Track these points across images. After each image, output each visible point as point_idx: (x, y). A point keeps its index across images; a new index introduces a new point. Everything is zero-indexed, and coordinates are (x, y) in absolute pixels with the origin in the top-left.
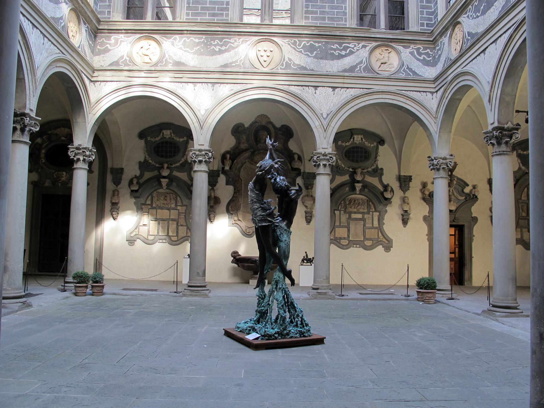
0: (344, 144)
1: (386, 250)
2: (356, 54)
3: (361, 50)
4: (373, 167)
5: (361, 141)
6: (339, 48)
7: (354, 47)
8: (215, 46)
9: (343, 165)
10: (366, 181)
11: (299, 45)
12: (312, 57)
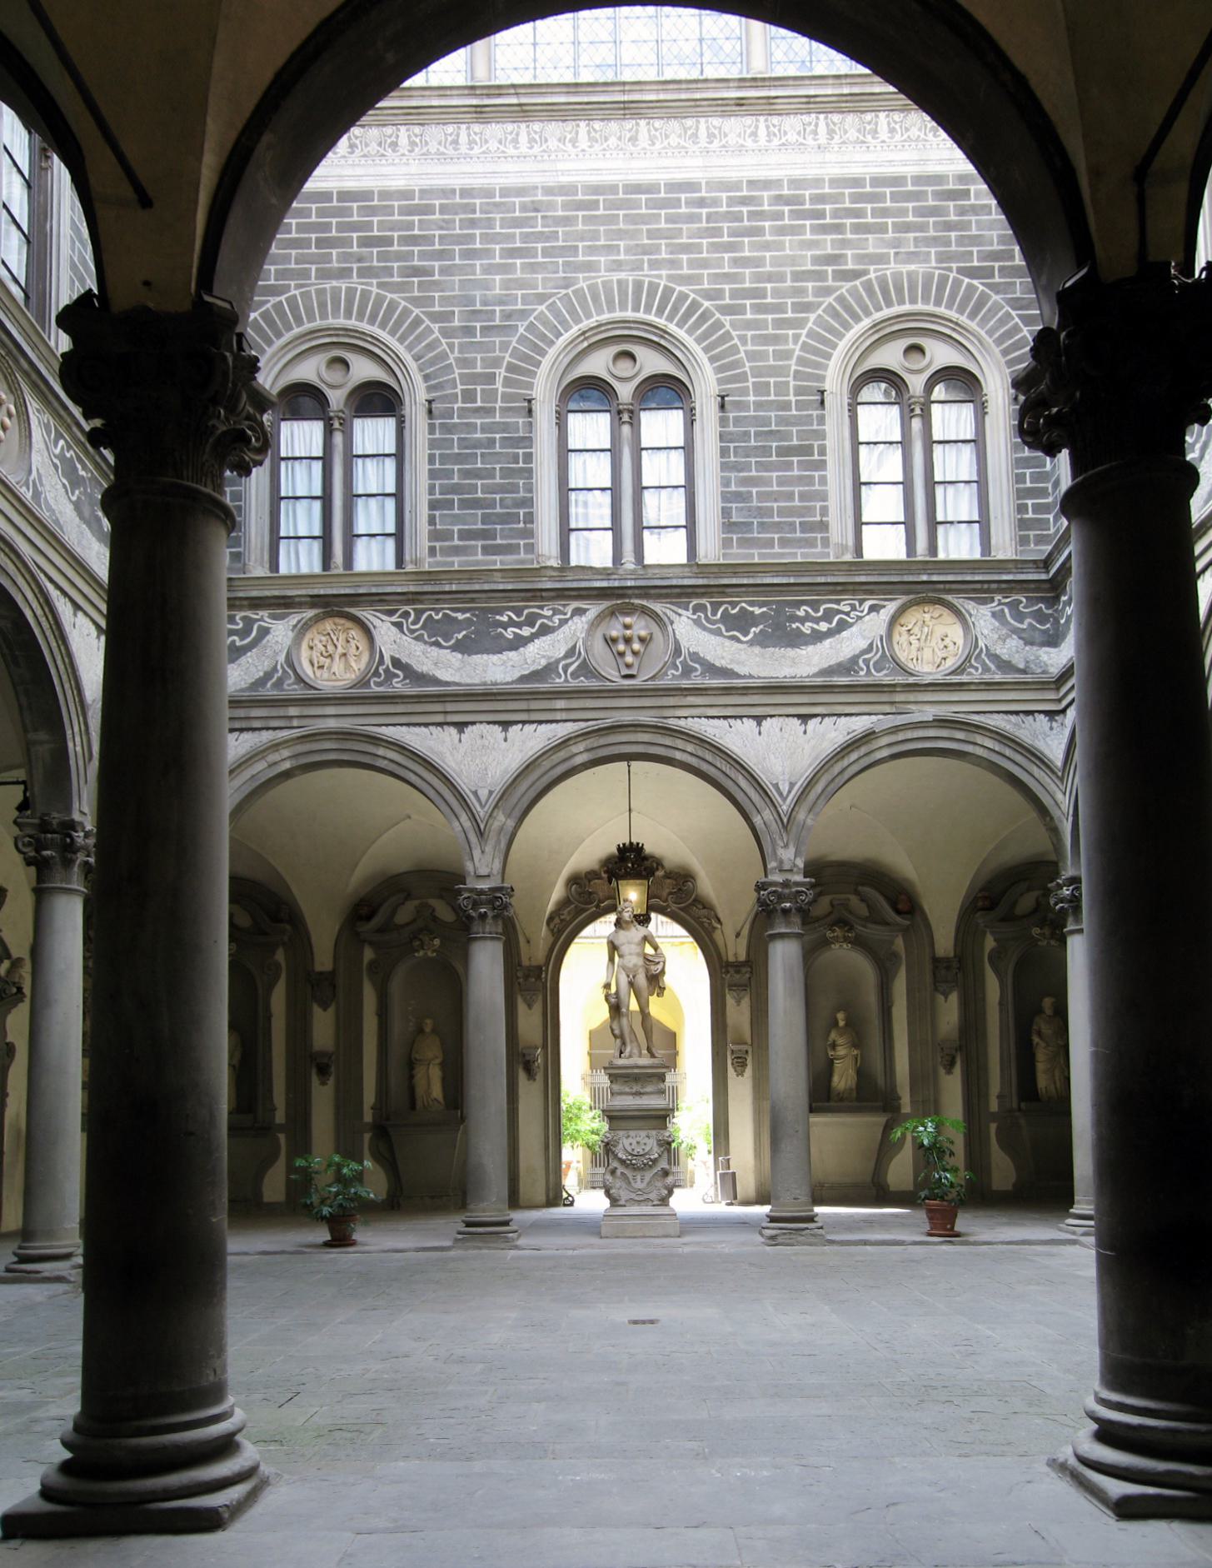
2: (854, 629)
3: (867, 617)
6: (813, 614)
7: (849, 612)
8: (505, 626)
11: (714, 613)
12: (747, 642)
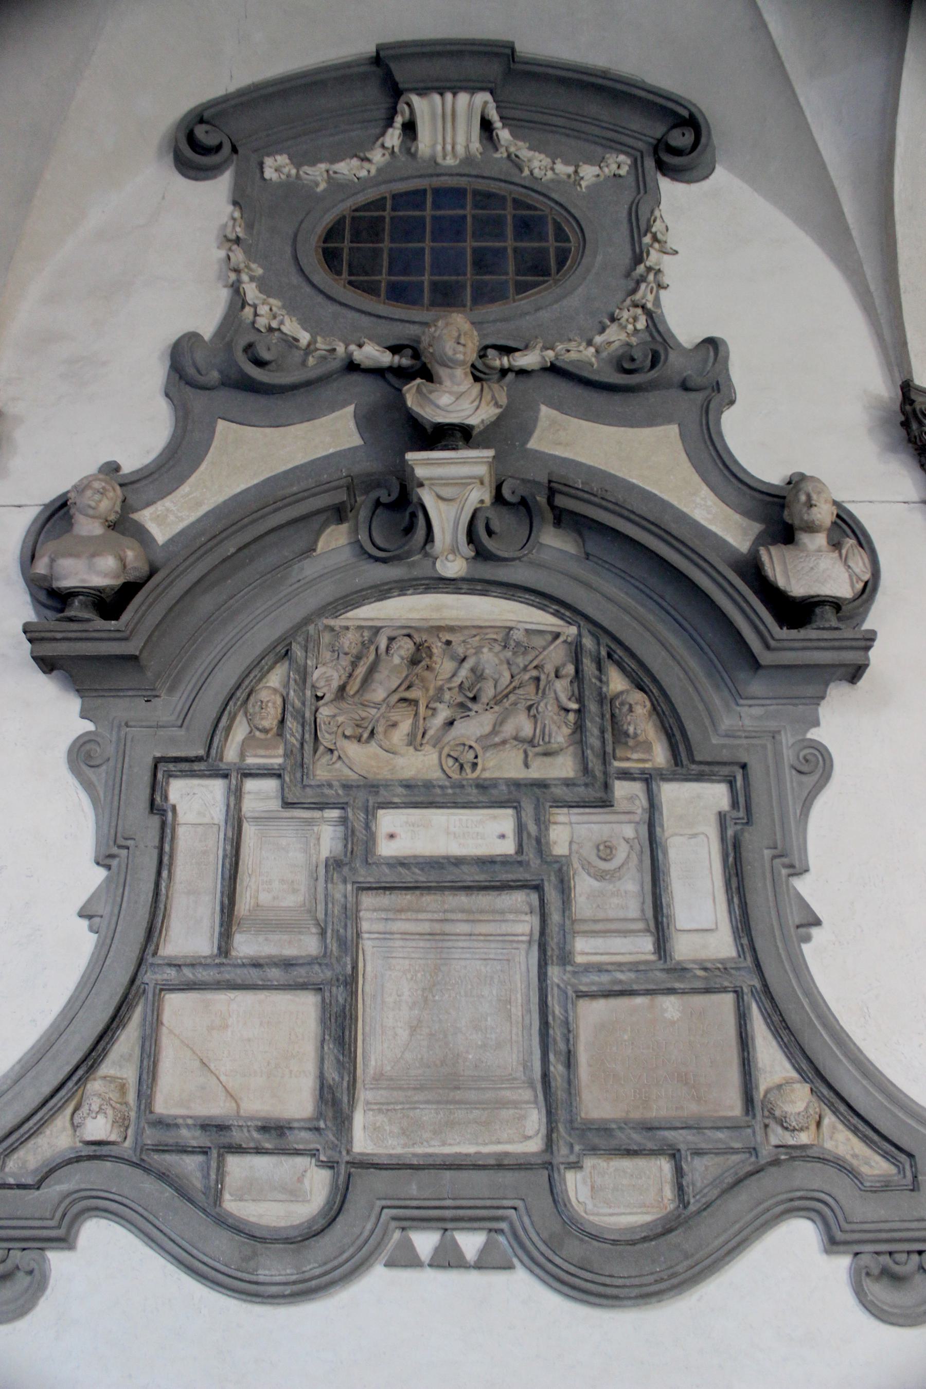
0: (316, 174)
1: (879, 1291)
4: (614, 337)
5: (476, 146)
9: (291, 327)
10: (538, 456)
